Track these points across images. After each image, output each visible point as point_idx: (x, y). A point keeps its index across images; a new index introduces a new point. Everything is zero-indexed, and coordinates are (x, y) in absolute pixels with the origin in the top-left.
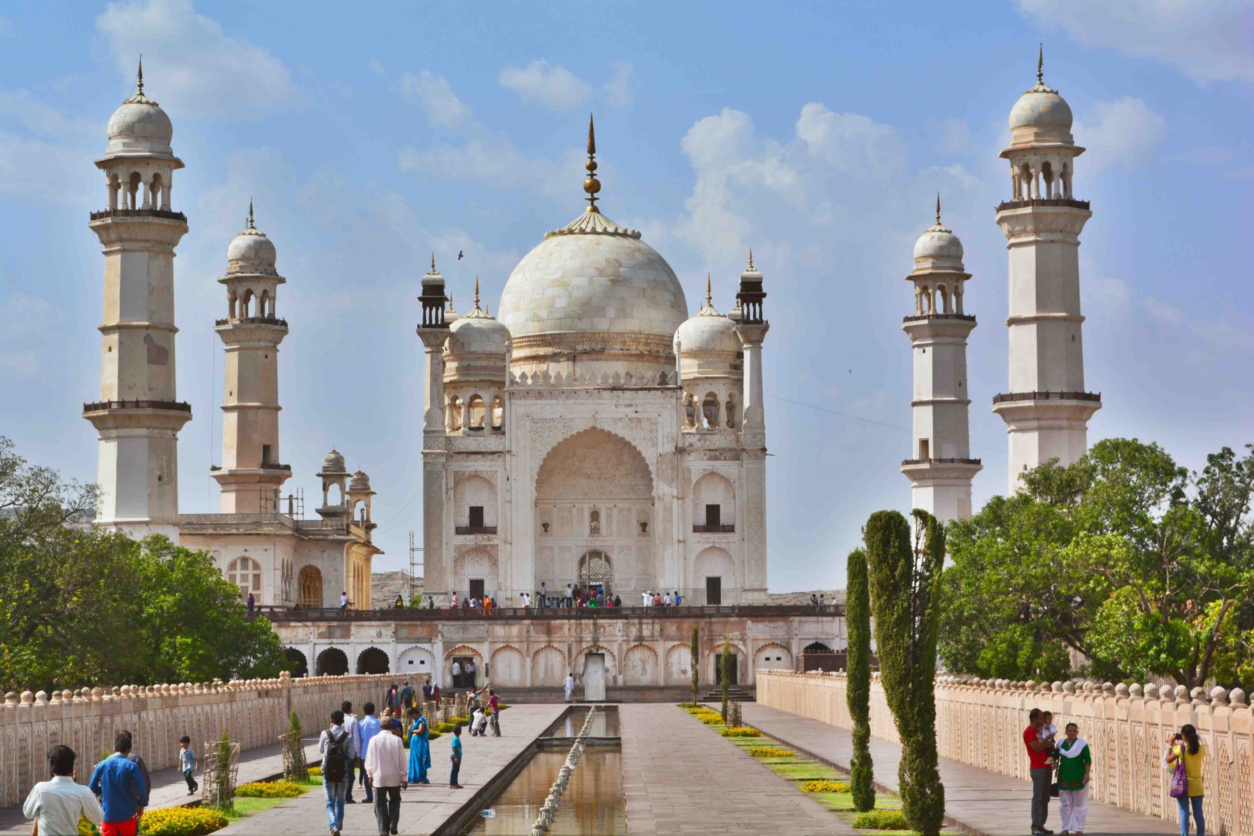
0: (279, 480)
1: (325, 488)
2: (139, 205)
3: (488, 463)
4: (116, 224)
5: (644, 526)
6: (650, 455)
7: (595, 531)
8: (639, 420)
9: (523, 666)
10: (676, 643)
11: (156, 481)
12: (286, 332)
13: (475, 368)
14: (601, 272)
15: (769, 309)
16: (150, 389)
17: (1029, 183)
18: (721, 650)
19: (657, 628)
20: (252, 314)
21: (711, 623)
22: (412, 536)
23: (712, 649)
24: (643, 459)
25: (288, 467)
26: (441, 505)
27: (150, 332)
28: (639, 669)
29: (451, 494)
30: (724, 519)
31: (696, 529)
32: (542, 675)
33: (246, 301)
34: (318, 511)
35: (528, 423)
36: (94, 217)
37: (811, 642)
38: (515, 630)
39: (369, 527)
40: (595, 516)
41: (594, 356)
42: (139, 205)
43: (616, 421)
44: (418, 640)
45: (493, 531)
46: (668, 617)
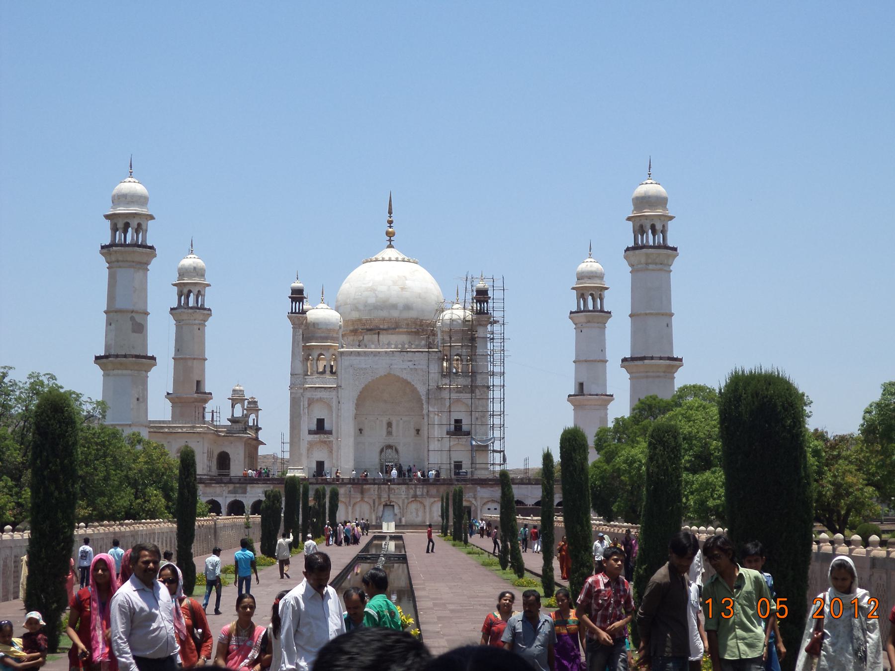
0: (205, 401)
1: (233, 407)
2: (128, 241)
3: (328, 393)
4: (116, 252)
5: (418, 431)
6: (422, 390)
7: (389, 433)
8: (416, 370)
12: (210, 315)
15: (494, 306)
17: (642, 236)
19: (425, 490)
20: (191, 305)
22: (283, 435)
24: (418, 392)
25: (210, 394)
26: (299, 416)
27: (133, 314)
28: (414, 514)
30: (465, 428)
33: (188, 296)
34: (228, 420)
36: (102, 247)
39: (257, 429)
40: (389, 425)
41: (390, 331)
42: (128, 241)
43: (402, 369)
45: (330, 433)
46: (431, 484)
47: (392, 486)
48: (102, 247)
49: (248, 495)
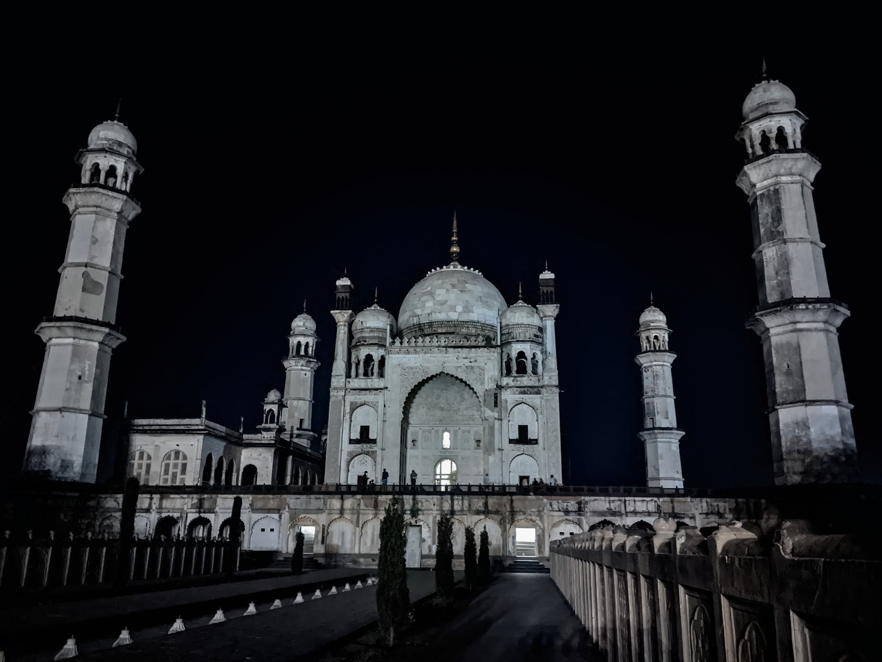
8: (472, 367)
9: (355, 533)
10: (482, 517)
11: (76, 379)
13: (369, 337)
16: (82, 310)
19: (466, 503)
21: (512, 501)
29: (347, 417)
30: (531, 435)
31: (511, 441)
32: (369, 544)
35: (399, 370)
37: (603, 519)
38: (349, 503)
44: (270, 511)
46: (475, 493)
47: (419, 497)
49: (217, 509)
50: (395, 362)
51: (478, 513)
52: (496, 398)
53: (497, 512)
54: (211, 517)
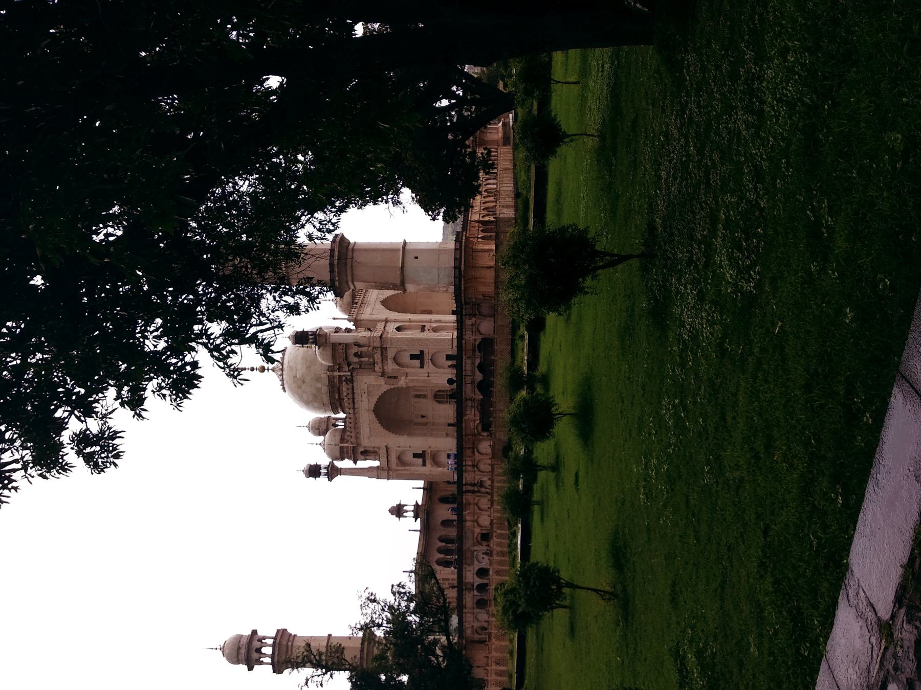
6: (385, 388)
14: (299, 387)
18: (480, 428)
23: (479, 434)
31: (422, 367)
48: (274, 672)
50: (366, 441)
51: (473, 453)
52: (391, 377)
53: (473, 444)
54: (476, 585)
